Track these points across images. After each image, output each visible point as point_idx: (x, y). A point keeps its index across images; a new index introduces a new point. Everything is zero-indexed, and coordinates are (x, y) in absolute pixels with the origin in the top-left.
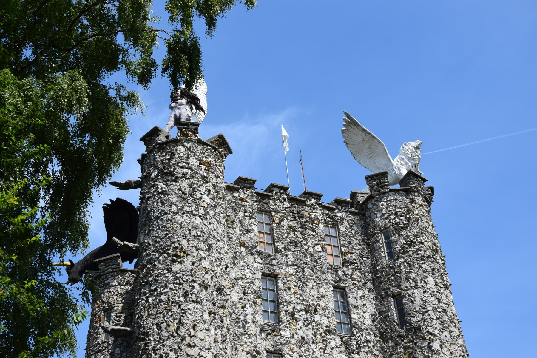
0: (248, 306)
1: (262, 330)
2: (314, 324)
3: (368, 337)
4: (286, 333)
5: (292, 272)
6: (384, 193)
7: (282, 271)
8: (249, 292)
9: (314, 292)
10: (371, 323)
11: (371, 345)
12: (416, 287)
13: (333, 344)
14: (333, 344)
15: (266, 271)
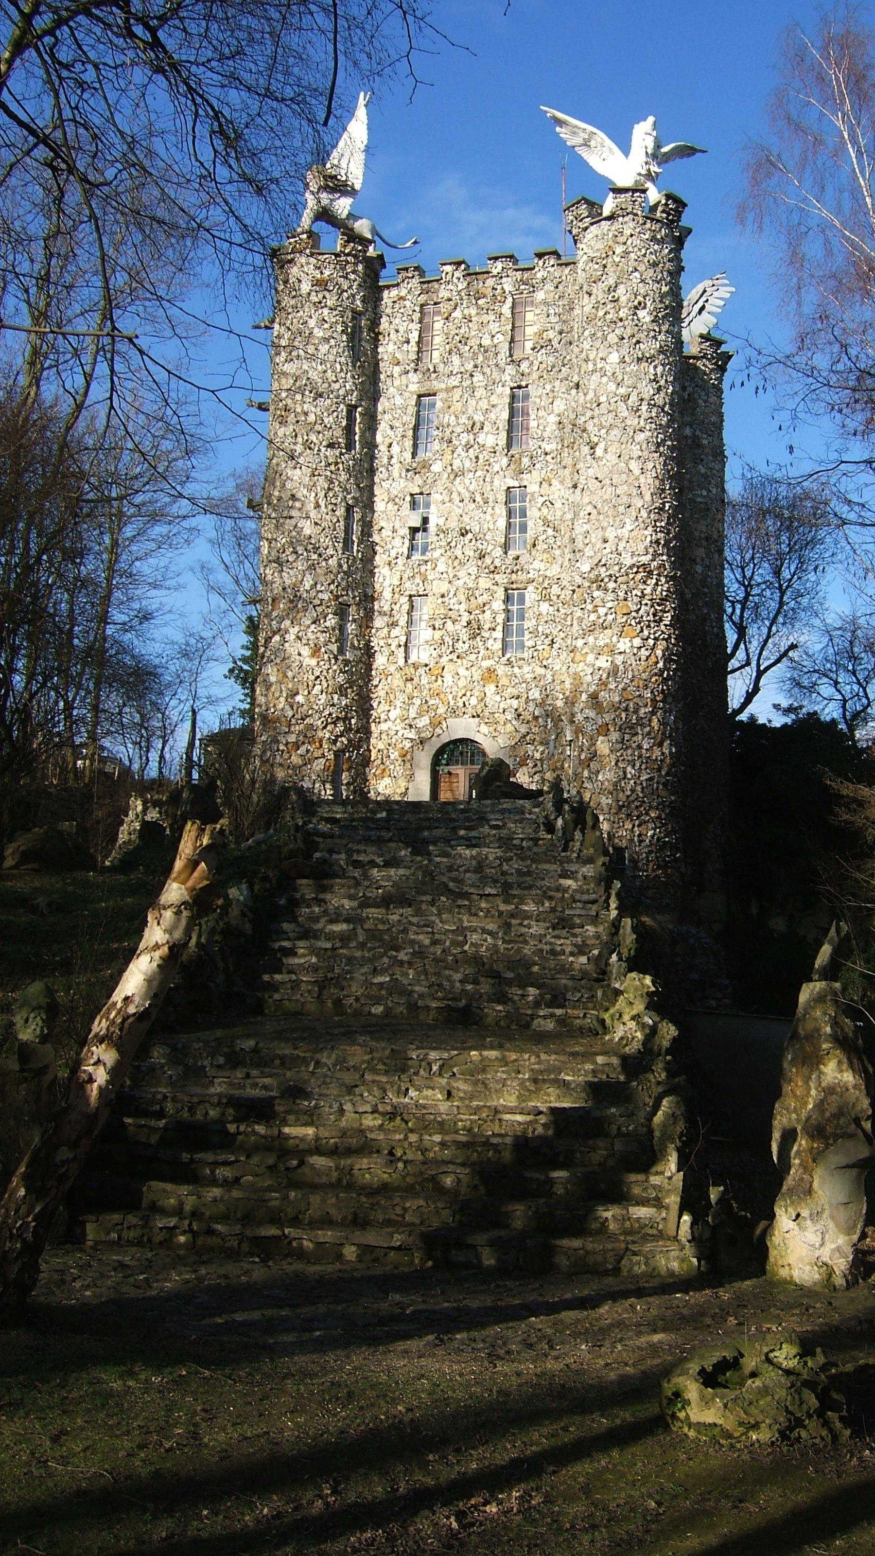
0: (395, 444)
1: (408, 470)
2: (476, 446)
3: (548, 450)
4: (437, 467)
5: (456, 383)
6: (586, 229)
7: (443, 386)
8: (397, 425)
9: (484, 404)
10: (554, 427)
11: (549, 458)
12: (594, 371)
13: (497, 468)
14: (497, 468)
15: (423, 391)
